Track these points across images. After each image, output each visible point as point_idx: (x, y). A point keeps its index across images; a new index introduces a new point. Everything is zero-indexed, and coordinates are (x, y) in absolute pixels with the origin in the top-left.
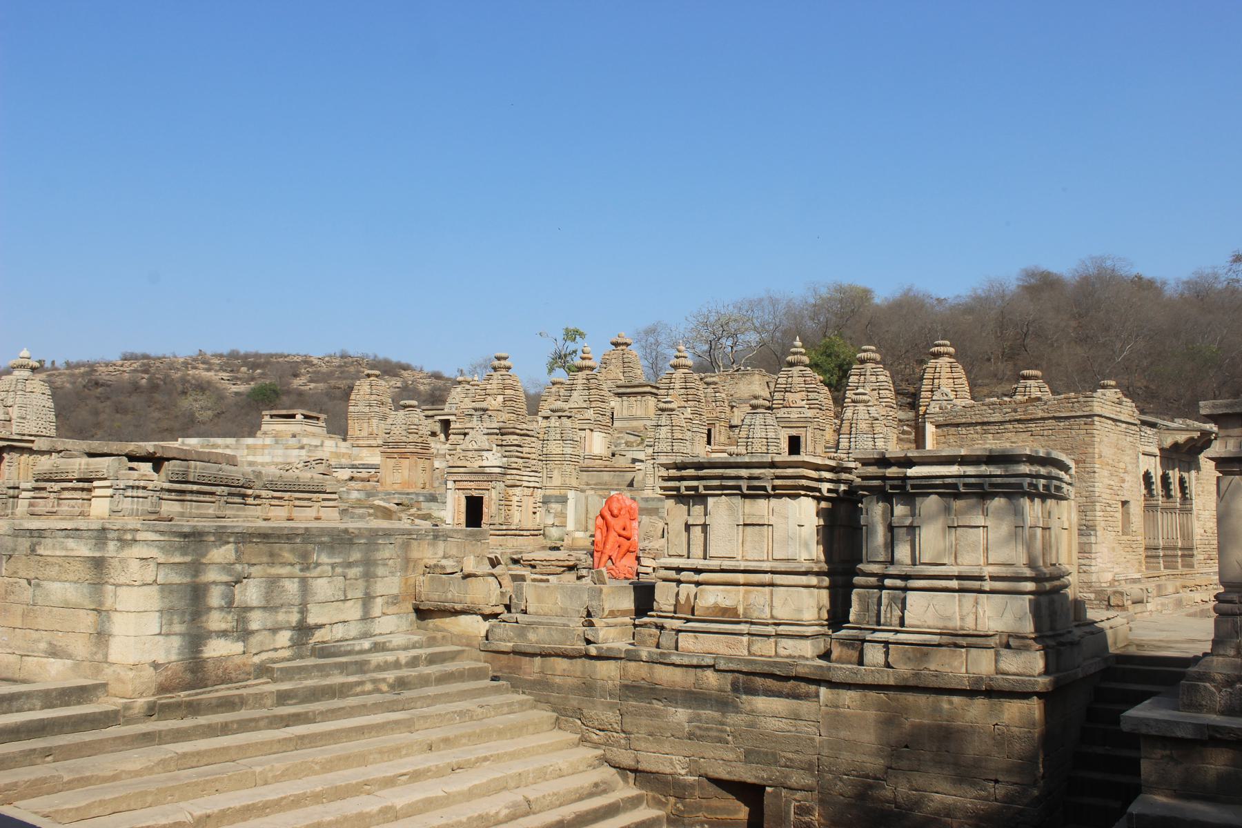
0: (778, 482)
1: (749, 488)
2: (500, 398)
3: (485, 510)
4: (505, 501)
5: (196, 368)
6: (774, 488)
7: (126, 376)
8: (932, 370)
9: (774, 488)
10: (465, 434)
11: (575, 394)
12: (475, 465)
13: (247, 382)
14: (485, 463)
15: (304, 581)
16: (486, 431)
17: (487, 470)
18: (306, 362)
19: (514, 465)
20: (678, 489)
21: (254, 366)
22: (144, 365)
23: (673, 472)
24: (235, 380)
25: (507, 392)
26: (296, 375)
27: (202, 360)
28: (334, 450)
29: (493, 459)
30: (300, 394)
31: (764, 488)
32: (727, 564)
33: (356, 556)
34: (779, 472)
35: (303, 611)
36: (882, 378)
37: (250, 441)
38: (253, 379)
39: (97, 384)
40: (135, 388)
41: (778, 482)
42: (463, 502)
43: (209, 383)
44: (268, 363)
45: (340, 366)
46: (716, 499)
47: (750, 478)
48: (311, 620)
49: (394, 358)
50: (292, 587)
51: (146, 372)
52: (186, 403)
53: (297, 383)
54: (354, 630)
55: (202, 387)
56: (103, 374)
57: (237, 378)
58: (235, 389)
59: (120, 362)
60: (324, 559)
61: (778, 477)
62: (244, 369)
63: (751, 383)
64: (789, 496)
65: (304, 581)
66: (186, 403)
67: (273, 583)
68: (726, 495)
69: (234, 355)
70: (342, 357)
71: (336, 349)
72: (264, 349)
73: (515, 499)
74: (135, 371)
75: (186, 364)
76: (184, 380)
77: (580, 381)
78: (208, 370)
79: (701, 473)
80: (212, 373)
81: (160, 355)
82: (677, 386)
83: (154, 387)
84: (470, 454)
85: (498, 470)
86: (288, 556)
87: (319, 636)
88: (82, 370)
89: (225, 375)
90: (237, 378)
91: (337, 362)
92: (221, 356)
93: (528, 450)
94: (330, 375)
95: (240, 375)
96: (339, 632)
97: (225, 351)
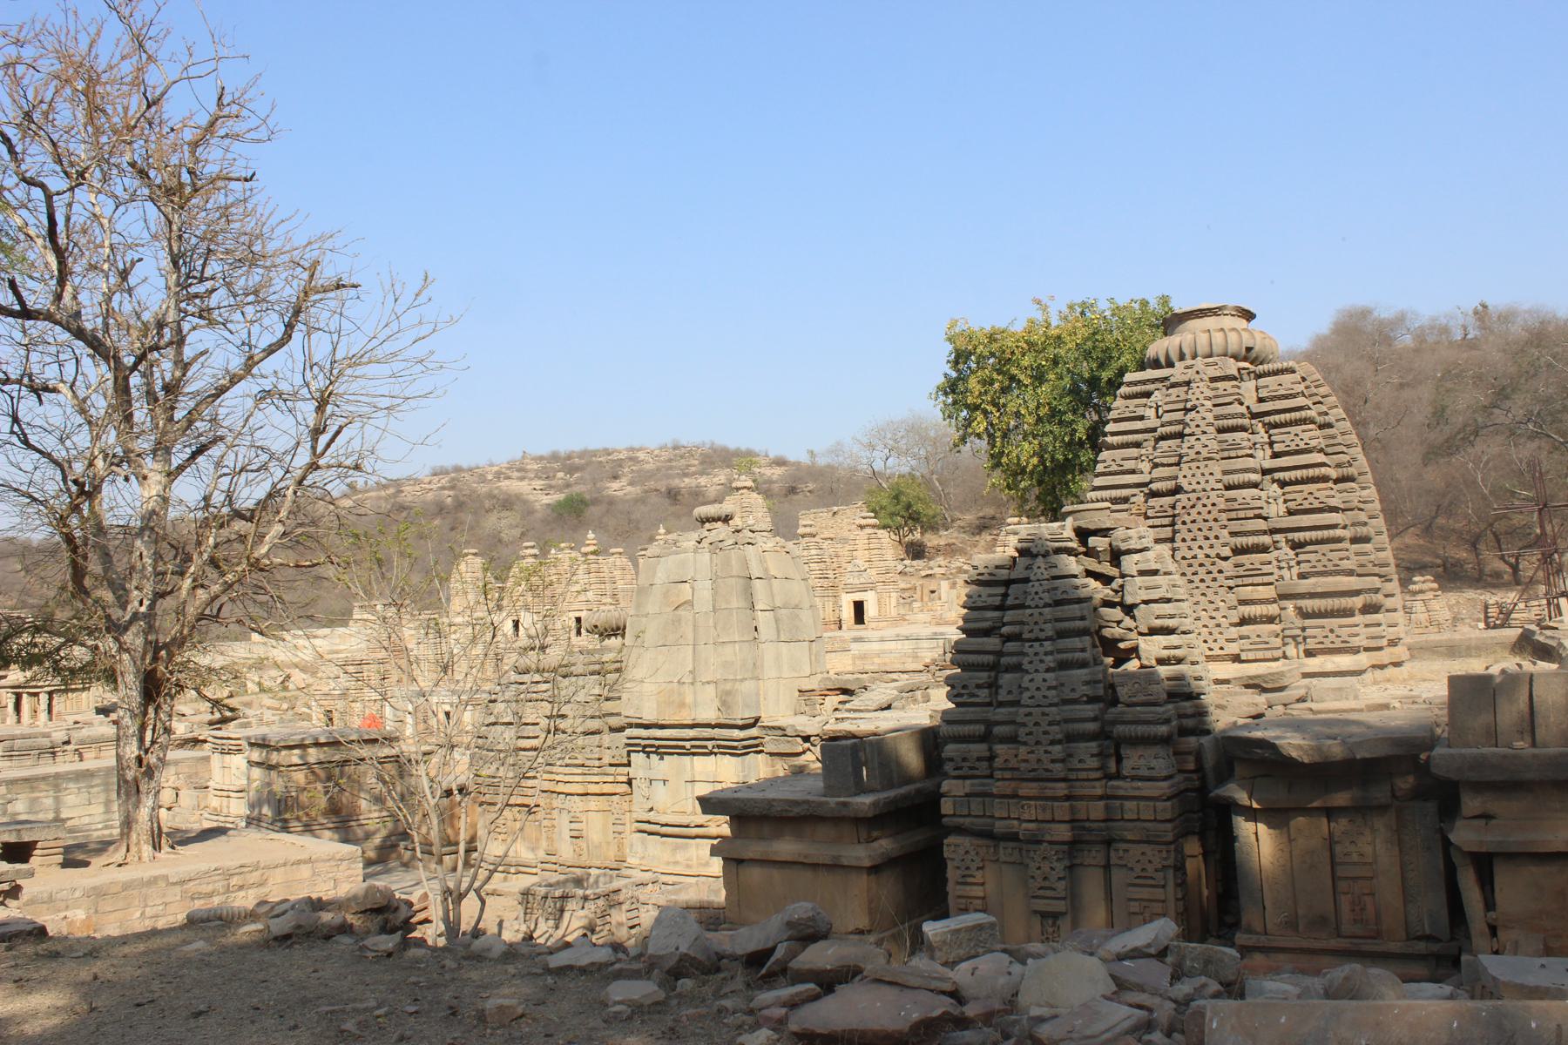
5: (509, 478)
7: (430, 496)
13: (560, 489)
15: (57, 799)
18: (631, 459)
21: (571, 470)
22: (453, 479)
24: (546, 490)
26: (615, 477)
27: (519, 469)
30: (611, 502)
33: (97, 781)
35: (57, 811)
37: (342, 630)
38: (568, 486)
39: (402, 508)
40: (441, 509)
43: (518, 497)
44: (589, 464)
45: (670, 460)
48: (63, 816)
49: (732, 445)
50: (49, 802)
51: (453, 488)
52: (492, 522)
53: (615, 488)
54: (98, 819)
55: (507, 503)
56: (409, 494)
57: (551, 487)
58: (546, 500)
59: (427, 480)
60: (71, 785)
62: (560, 475)
65: (57, 799)
66: (492, 522)
67: (34, 801)
69: (555, 457)
70: (675, 448)
71: (668, 440)
72: (594, 444)
74: (443, 488)
75: (498, 475)
76: (491, 496)
78: (522, 479)
80: (525, 483)
81: (473, 465)
83: (459, 505)
86: (43, 787)
87: (69, 823)
88: (391, 491)
89: (538, 484)
90: (551, 487)
91: (665, 455)
92: (541, 458)
94: (651, 475)
95: (553, 483)
96: (86, 820)
97: (544, 450)
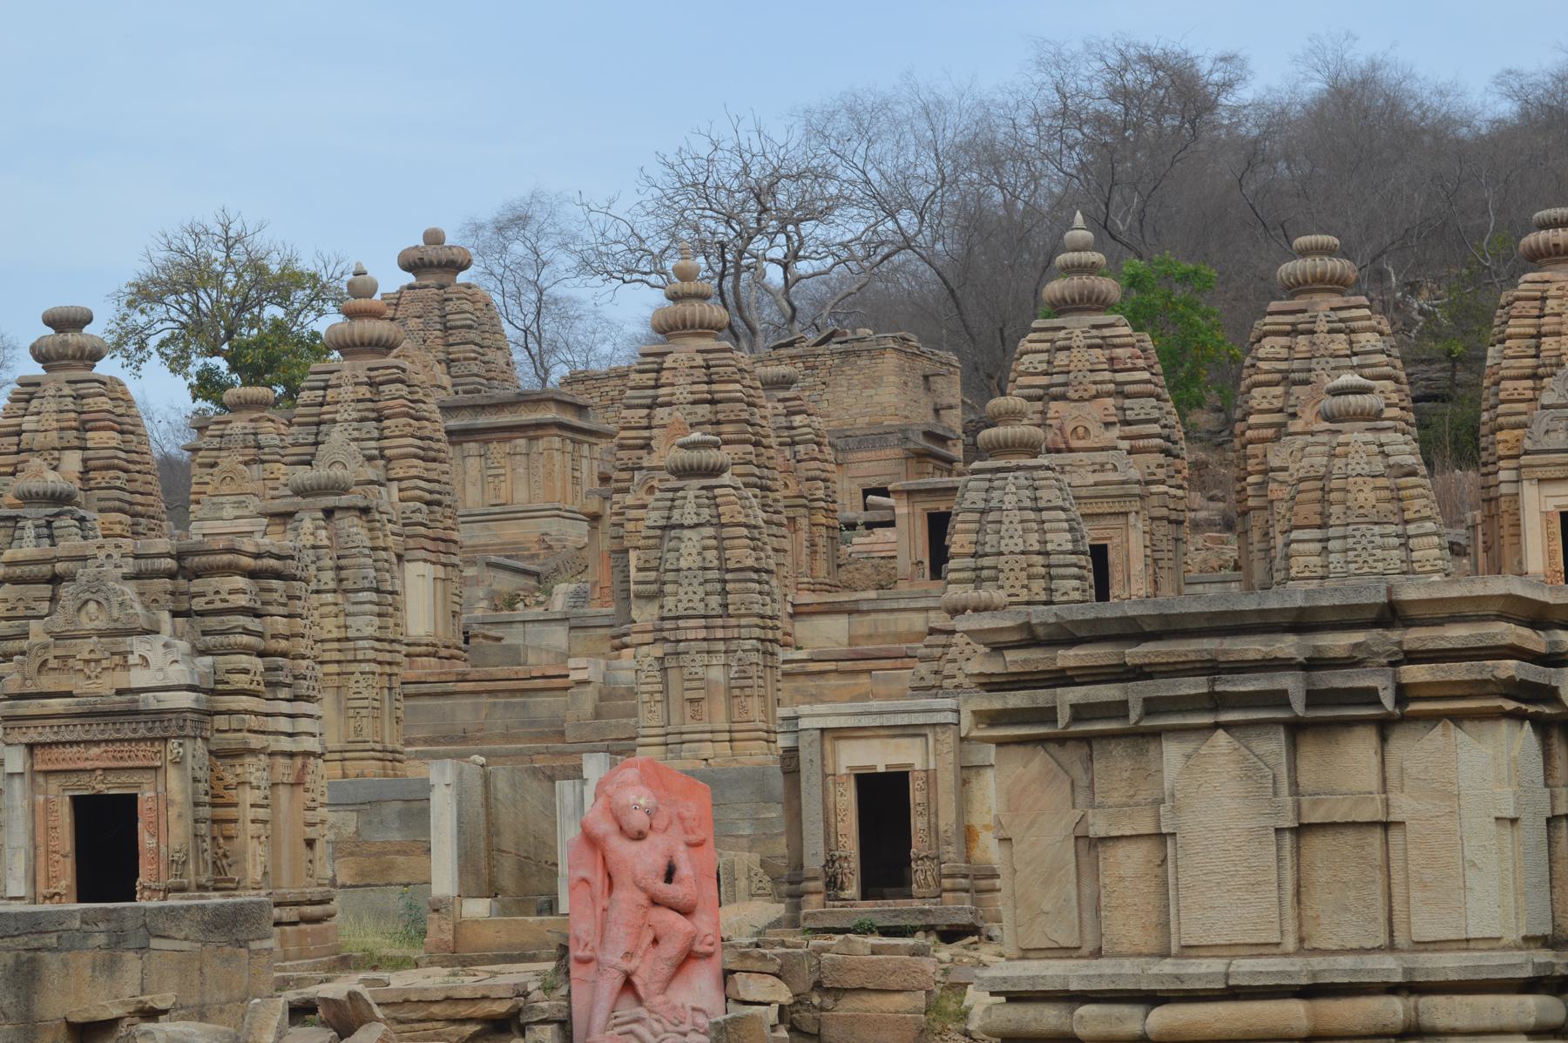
0: (1416, 674)
1: (1315, 698)
3: (146, 841)
4: (215, 807)
6: (1403, 694)
8: (1531, 308)
9: (1403, 694)
10: (55, 580)
11: (337, 436)
12: (107, 684)
14: (138, 678)
16: (129, 566)
17: (150, 701)
19: (240, 681)
20: (1046, 715)
23: (1016, 660)
25: (94, 438)
29: (163, 666)
31: (1369, 697)
32: (1247, 969)
34: (1415, 637)
36: (1368, 340)
41: (1416, 674)
42: (64, 817)
46: (1188, 747)
47: (1314, 664)
61: (1413, 657)
63: (876, 381)
64: (1457, 718)
68: (1227, 727)
73: (248, 796)
77: (347, 392)
79: (1137, 654)
82: (682, 393)
84: (84, 649)
85: (185, 700)
93: (281, 625)
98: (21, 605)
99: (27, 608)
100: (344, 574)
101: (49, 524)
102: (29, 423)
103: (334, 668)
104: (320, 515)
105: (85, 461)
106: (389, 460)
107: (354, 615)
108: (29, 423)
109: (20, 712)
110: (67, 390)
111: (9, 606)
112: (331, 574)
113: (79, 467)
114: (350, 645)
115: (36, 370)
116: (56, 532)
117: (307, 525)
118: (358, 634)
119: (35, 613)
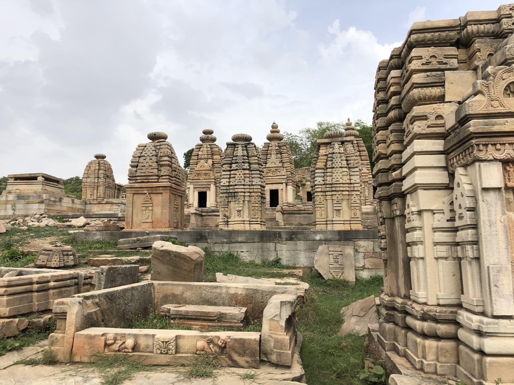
2: (210, 162)
25: (215, 157)
28: (71, 205)
77: (274, 148)
98: (434, 61)
99: (440, 63)
100: (349, 162)
101: (246, 146)
102: (200, 153)
103: (347, 193)
104: (340, 143)
105: (213, 162)
106: (283, 163)
107: (353, 175)
108: (200, 153)
109: (496, 128)
110: (209, 146)
111: (424, 61)
112: (345, 162)
113: (211, 163)
114: (352, 185)
115: (201, 143)
116: (249, 149)
117: (336, 146)
118: (355, 182)
119: (448, 66)
